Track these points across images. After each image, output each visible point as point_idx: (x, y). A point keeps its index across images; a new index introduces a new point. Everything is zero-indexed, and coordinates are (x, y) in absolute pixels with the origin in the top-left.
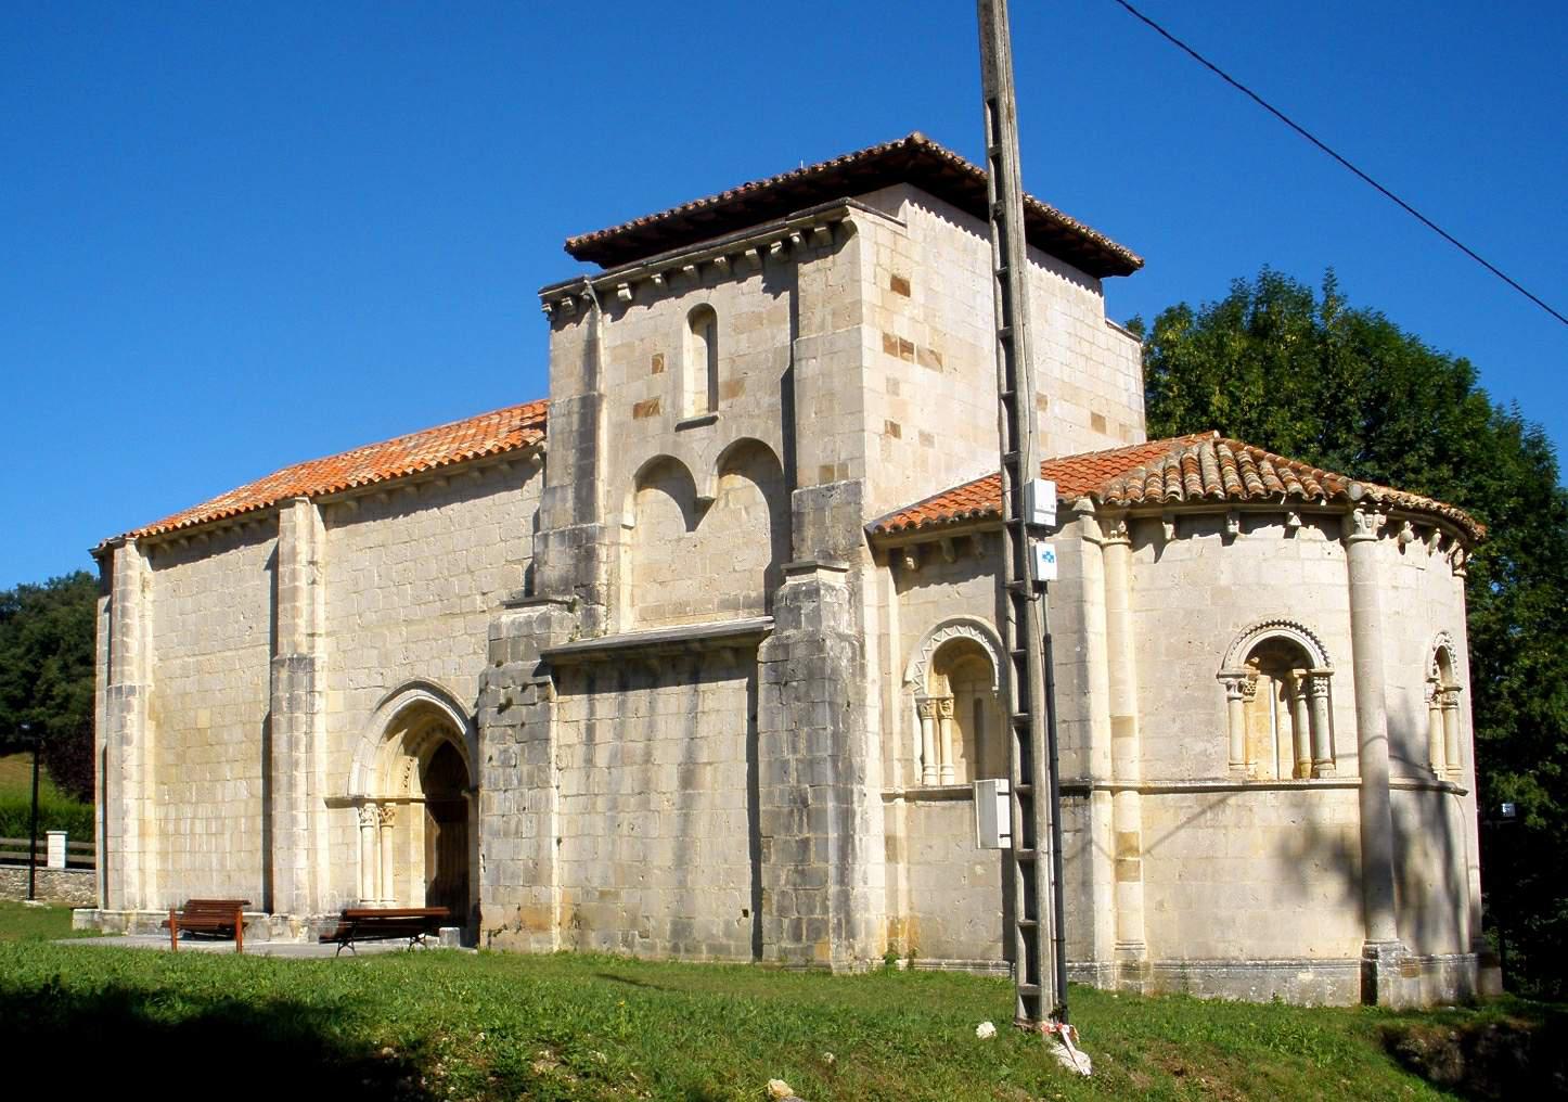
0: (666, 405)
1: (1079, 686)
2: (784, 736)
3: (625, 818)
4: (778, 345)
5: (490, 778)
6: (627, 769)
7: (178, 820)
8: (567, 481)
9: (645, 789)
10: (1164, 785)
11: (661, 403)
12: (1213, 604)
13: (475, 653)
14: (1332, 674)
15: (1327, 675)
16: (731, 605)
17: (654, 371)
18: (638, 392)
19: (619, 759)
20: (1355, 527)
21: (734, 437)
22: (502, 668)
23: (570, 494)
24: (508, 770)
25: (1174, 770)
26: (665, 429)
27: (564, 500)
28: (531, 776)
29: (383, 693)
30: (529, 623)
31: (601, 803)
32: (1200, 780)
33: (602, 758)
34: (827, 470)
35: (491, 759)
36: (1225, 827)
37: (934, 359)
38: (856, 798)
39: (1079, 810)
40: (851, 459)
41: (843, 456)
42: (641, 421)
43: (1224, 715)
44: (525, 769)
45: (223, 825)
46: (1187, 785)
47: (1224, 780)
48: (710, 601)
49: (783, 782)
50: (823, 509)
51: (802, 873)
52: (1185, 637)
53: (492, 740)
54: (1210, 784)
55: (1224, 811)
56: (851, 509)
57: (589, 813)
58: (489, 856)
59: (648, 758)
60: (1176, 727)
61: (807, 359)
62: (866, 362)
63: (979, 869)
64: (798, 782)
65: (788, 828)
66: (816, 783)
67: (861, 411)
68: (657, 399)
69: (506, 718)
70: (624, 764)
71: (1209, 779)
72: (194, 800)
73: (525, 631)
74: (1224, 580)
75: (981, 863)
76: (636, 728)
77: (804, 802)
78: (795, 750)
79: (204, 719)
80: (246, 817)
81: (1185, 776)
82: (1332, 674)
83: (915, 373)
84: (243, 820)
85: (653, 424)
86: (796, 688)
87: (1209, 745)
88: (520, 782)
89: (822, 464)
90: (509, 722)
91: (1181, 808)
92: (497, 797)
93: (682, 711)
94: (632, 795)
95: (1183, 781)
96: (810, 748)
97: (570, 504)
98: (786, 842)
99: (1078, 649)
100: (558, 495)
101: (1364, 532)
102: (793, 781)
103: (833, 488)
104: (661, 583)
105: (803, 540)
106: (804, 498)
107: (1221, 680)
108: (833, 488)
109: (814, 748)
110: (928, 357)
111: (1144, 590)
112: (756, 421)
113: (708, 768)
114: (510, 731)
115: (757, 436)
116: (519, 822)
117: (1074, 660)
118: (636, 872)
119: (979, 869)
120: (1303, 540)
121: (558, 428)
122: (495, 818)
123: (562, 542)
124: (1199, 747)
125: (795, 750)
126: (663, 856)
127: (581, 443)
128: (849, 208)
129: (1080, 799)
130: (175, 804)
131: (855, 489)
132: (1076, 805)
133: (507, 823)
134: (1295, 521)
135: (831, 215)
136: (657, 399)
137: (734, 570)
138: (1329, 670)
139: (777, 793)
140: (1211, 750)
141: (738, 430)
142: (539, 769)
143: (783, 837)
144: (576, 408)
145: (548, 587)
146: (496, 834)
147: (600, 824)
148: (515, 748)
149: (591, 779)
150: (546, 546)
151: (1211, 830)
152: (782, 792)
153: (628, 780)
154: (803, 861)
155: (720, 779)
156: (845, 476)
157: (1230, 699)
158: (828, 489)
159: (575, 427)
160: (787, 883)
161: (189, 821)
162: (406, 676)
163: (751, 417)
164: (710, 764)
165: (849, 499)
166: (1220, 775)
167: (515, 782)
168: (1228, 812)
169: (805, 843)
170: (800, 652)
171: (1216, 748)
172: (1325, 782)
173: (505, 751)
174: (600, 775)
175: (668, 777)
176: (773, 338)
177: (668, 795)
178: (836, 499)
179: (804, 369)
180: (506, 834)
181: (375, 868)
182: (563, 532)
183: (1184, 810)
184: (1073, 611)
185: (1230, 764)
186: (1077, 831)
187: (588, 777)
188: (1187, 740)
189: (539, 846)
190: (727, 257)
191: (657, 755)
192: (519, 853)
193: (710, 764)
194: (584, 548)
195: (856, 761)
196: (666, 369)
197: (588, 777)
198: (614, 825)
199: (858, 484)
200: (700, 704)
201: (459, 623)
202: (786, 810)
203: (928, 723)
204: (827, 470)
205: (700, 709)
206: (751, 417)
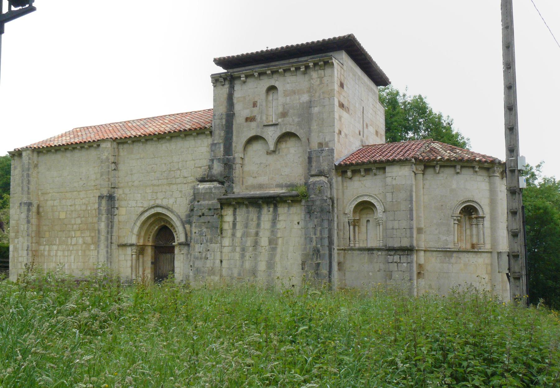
0: (258, 118)
1: (410, 218)
2: (311, 230)
3: (248, 255)
4: (301, 101)
5: (194, 239)
6: (249, 238)
7: (49, 251)
8: (221, 141)
9: (256, 244)
11: (257, 117)
13: (182, 197)
14: (485, 217)
15: (483, 218)
16: (280, 186)
17: (254, 107)
18: (246, 113)
19: (245, 235)
20: (494, 172)
21: (284, 131)
22: (200, 203)
23: (222, 146)
24: (202, 237)
25: (436, 245)
26: (258, 126)
27: (220, 148)
28: (211, 239)
29: (142, 209)
30: (211, 189)
31: (238, 249)
32: (444, 248)
33: (239, 234)
34: (320, 144)
35: (195, 233)
37: (347, 110)
38: (332, 249)
39: (409, 257)
40: (330, 141)
41: (327, 140)
42: (249, 123)
43: (452, 229)
44: (209, 237)
45: (71, 253)
47: (452, 249)
48: (272, 184)
49: (310, 244)
50: (319, 157)
51: (317, 274)
53: (195, 227)
54: (448, 250)
56: (330, 157)
57: (233, 252)
58: (194, 266)
59: (257, 234)
60: (437, 231)
61: (314, 107)
62: (336, 110)
63: (371, 274)
64: (316, 244)
65: (312, 259)
66: (323, 245)
67: (334, 126)
68: (256, 116)
69: (203, 219)
70: (247, 236)
72: (57, 243)
73: (208, 191)
74: (454, 186)
75: (372, 272)
76: (253, 224)
77: (318, 251)
78: (315, 234)
79: (62, 216)
80: (81, 250)
82: (485, 217)
83: (345, 114)
84: (80, 251)
85: (253, 124)
86: (316, 215)
88: (207, 241)
89: (319, 142)
90: (203, 221)
92: (197, 246)
93: (270, 220)
94: (251, 246)
96: (321, 234)
97: (222, 149)
98: (311, 263)
99: (410, 206)
100: (217, 146)
102: (314, 244)
103: (323, 150)
104: (253, 177)
105: (311, 166)
106: (312, 152)
108: (323, 150)
109: (323, 234)
110: (347, 109)
112: (292, 126)
113: (280, 239)
114: (203, 224)
115: (293, 131)
116: (206, 254)
117: (408, 209)
118: (254, 272)
119: (371, 274)
121: (217, 123)
122: (197, 253)
123: (219, 162)
124: (444, 238)
125: (315, 234)
126: (262, 266)
127: (226, 129)
128: (333, 58)
129: (409, 253)
130: (49, 245)
131: (332, 151)
132: (408, 255)
133: (202, 255)
134: (477, 169)
135: (326, 59)
136: (255, 116)
137: (281, 175)
138: (484, 216)
139: (308, 247)
140: (448, 239)
141: (286, 129)
142: (215, 237)
143: (310, 262)
144: (224, 117)
145: (213, 176)
146: (197, 258)
147: (237, 256)
148: (205, 230)
149: (234, 241)
150: (213, 163)
151: (447, 264)
152: (310, 248)
153: (249, 242)
154: (317, 270)
155: (285, 242)
156: (327, 146)
157: (454, 223)
158: (321, 150)
159: (224, 123)
160: (311, 276)
161: (55, 251)
162: (152, 203)
163: (291, 125)
164: (281, 237)
165: (329, 154)
166: (451, 247)
167: (205, 241)
168: (453, 258)
169: (318, 265)
170: (318, 203)
172: (483, 250)
173: (201, 231)
174: (237, 240)
175: (264, 241)
176: (299, 99)
177: (264, 247)
178: (324, 154)
179: (313, 110)
180: (201, 258)
181: (136, 268)
182: (220, 158)
184: (409, 194)
186: (409, 263)
187: (233, 240)
189: (214, 262)
190: (283, 70)
191: (261, 234)
192: (206, 265)
193: (281, 237)
194: (228, 165)
195: (332, 238)
196: (258, 106)
197: (233, 240)
198: (243, 256)
199: (333, 150)
200: (277, 218)
201: (175, 187)
202: (311, 253)
203: (352, 227)
204: (320, 144)
205: (277, 219)
206: (291, 125)
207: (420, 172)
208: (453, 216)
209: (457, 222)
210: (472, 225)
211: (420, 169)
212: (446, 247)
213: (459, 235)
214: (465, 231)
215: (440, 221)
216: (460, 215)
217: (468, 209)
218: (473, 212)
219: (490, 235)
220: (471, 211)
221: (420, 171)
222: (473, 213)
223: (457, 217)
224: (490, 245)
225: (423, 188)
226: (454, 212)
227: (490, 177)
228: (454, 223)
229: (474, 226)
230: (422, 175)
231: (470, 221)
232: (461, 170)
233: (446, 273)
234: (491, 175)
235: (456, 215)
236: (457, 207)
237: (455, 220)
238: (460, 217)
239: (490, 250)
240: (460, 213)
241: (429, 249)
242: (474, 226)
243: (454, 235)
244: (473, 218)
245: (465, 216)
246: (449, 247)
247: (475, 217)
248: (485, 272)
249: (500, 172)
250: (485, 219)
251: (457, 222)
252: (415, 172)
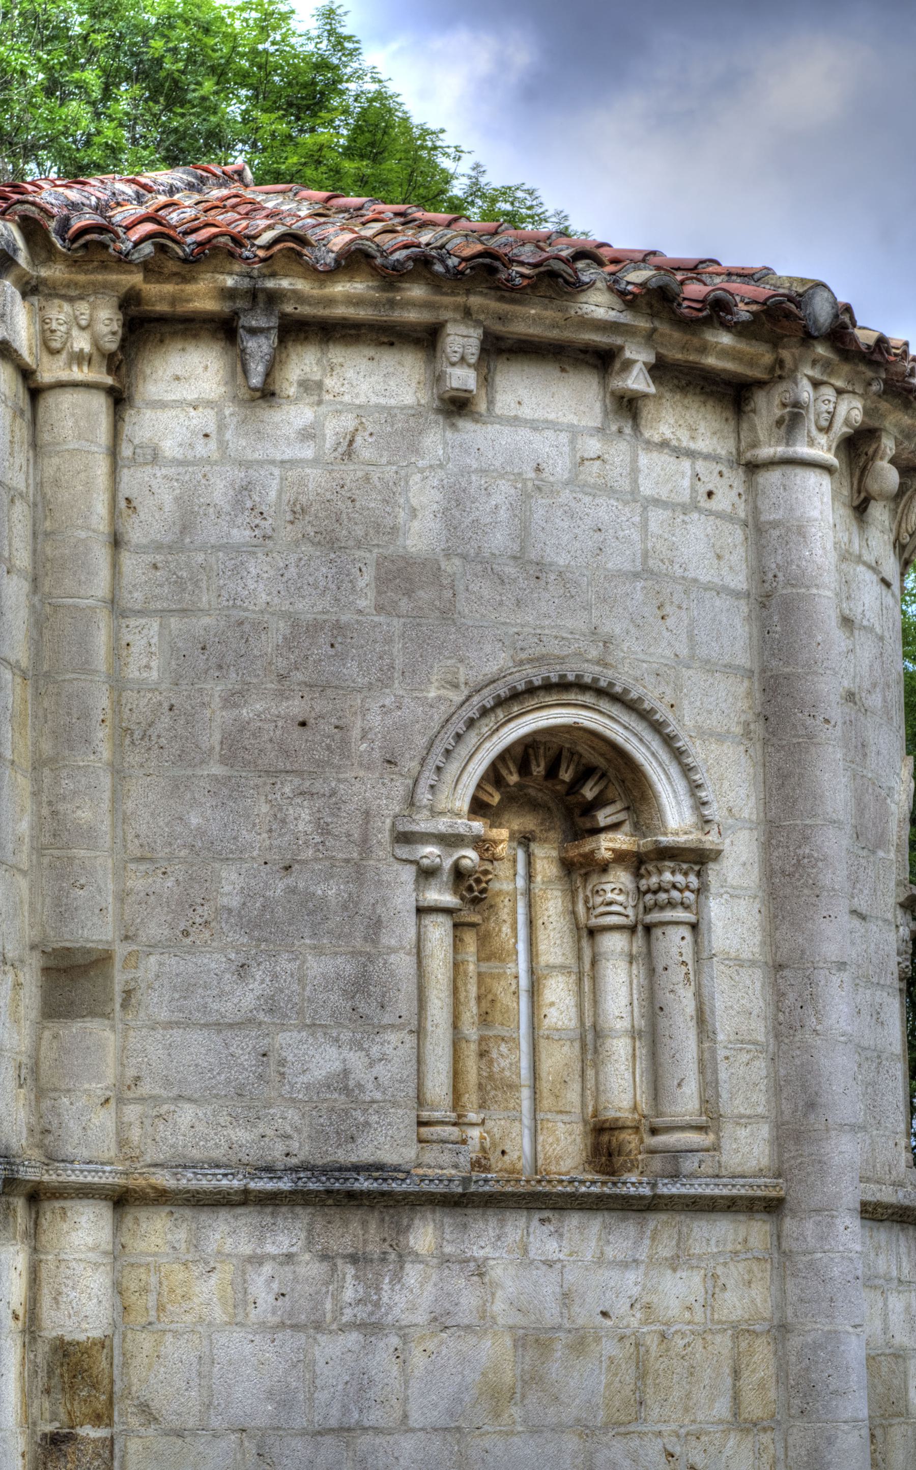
10: (205, 1184)
12: (380, 608)
25: (241, 1135)
36: (403, 1332)
43: (404, 963)
46: (285, 1185)
52: (296, 707)
54: (364, 1184)
55: (397, 1277)
71: (357, 1168)
81: (276, 1152)
87: (356, 1060)
91: (257, 1260)
95: (269, 1169)
101: (812, 443)
107: (403, 852)
111: (158, 547)
120: (649, 445)
138: (711, 840)
140: (360, 1072)
157: (422, 911)
166: (389, 1157)
168: (412, 1274)
171: (379, 1069)
183: (267, 1269)
185: (421, 1124)
188: (282, 1038)
207: (79, 374)
208: (405, 838)
209: (448, 899)
210: (593, 933)
211: (82, 343)
212: (343, 1156)
213: (471, 1031)
214: (534, 991)
215: (279, 887)
216: (478, 826)
217: (552, 772)
218: (600, 802)
219: (759, 1031)
220: (589, 792)
221: (79, 358)
222: (603, 817)
223: (450, 841)
224: (765, 1131)
225: (116, 542)
226: (424, 796)
227: (753, 468)
228: (422, 911)
229: (614, 943)
230: (99, 403)
231: (573, 894)
232: (486, 381)
233: (343, 1430)
234: (766, 452)
235: (442, 825)
236: (447, 739)
237: (427, 874)
238: (480, 843)
239: (763, 1188)
240: (478, 807)
241: (164, 1179)
242: (614, 943)
243: (419, 1032)
244: (604, 868)
245: (525, 840)
246: (364, 1154)
247: (620, 857)
248: (722, 1408)
249: (840, 429)
250: (713, 872)
251: (448, 899)
252: (26, 374)
